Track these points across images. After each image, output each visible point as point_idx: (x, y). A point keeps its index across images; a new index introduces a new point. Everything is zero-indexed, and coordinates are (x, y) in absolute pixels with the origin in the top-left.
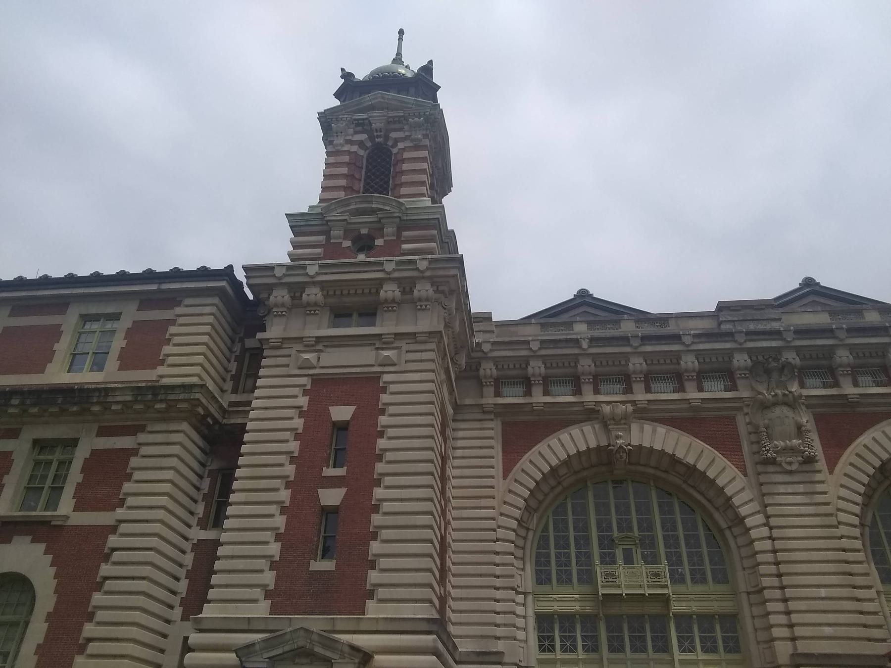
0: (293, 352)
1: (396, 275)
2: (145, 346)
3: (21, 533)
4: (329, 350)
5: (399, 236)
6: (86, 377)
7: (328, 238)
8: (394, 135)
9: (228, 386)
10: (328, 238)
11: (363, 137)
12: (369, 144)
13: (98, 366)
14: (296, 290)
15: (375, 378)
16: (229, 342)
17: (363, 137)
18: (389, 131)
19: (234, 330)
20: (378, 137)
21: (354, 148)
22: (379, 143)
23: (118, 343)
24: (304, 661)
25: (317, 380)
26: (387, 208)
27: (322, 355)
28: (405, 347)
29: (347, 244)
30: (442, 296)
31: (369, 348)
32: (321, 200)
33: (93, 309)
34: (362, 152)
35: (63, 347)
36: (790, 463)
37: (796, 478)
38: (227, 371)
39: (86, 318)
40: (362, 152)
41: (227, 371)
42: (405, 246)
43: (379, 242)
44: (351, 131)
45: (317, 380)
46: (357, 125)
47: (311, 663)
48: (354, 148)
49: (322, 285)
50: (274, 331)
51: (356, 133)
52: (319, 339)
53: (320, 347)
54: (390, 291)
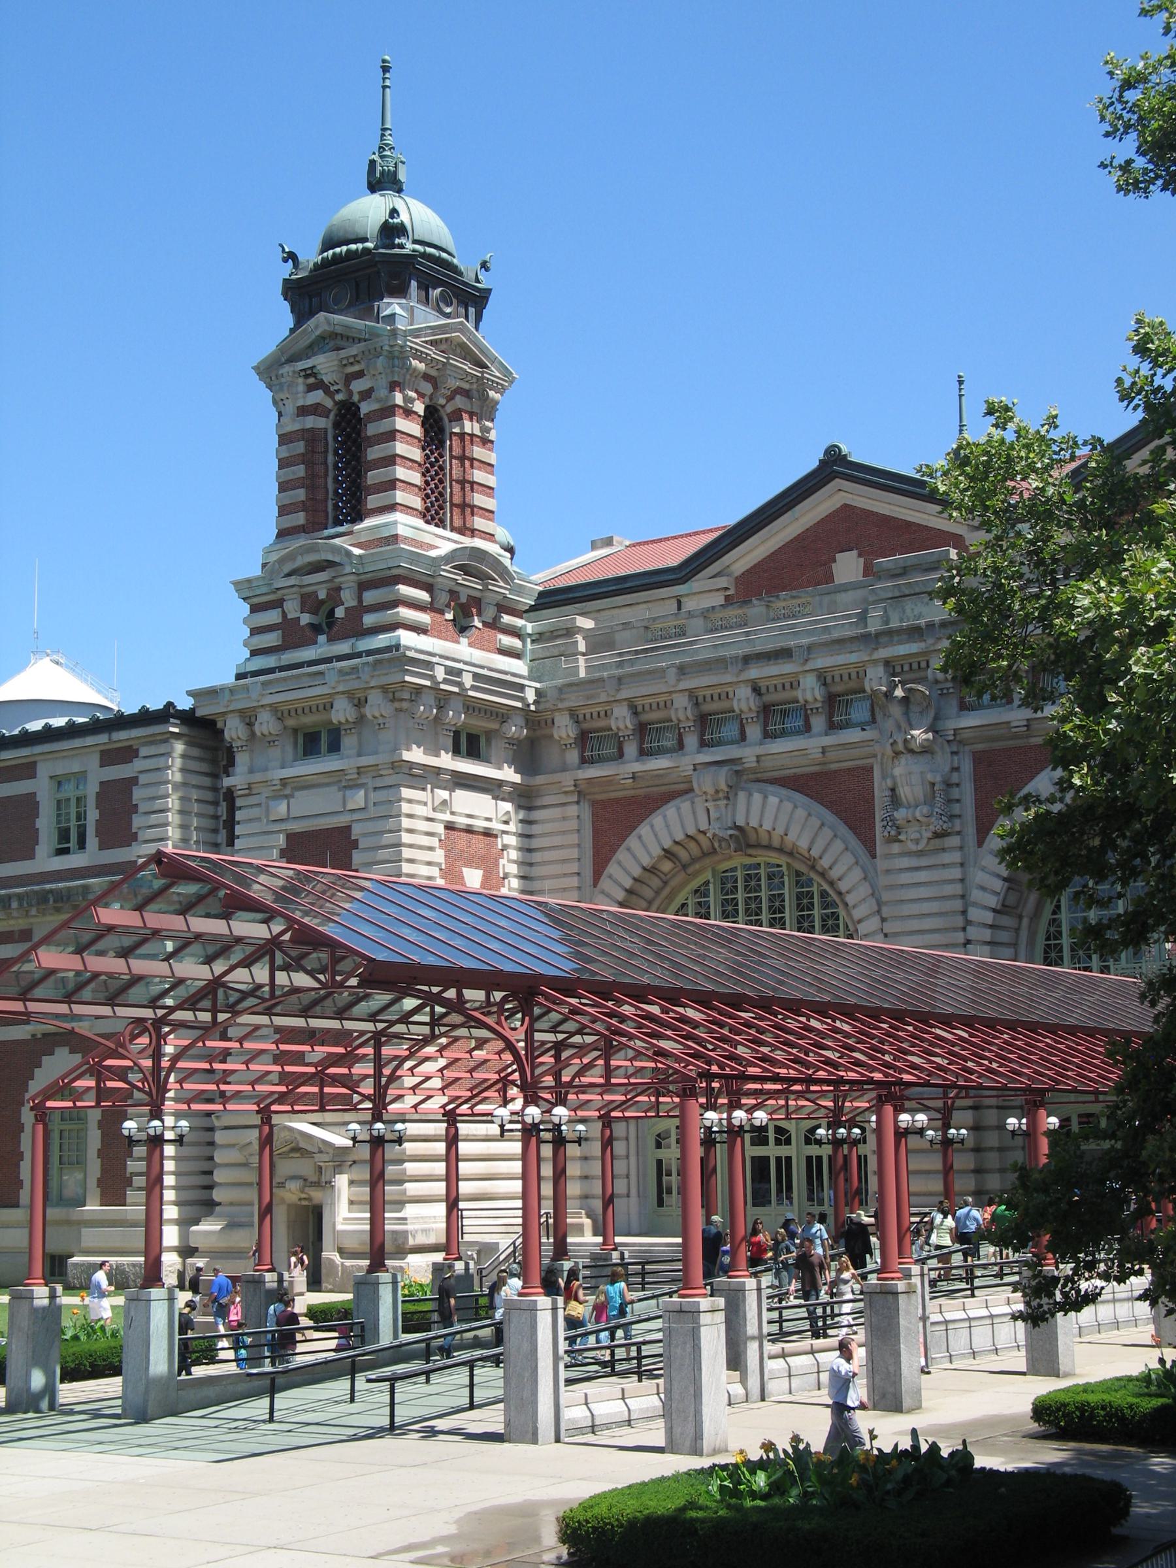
0: (261, 799)
1: (341, 688)
2: (119, 812)
3: (62, 1044)
4: (297, 794)
5: (360, 600)
6: (76, 860)
7: (284, 614)
8: (358, 386)
9: (222, 837)
10: (284, 614)
11: (317, 396)
12: (329, 403)
13: (82, 845)
14: (248, 718)
15: (348, 829)
16: (207, 781)
17: (317, 396)
18: (350, 378)
19: (214, 762)
20: (338, 391)
21: (310, 422)
22: (341, 402)
23: (93, 815)
24: (298, 1155)
25: (291, 837)
26: (337, 559)
27: (292, 800)
28: (371, 783)
29: (305, 619)
30: (405, 705)
31: (336, 788)
32: (282, 534)
33: (61, 768)
34: (321, 423)
35: (46, 824)
36: (917, 841)
37: (924, 862)
38: (216, 817)
39: (59, 781)
40: (321, 423)
41: (216, 817)
42: (369, 620)
43: (340, 613)
44: (301, 388)
45: (291, 837)
46: (307, 376)
47: (302, 1156)
48: (310, 422)
49: (274, 708)
50: (235, 780)
51: (310, 388)
52: (284, 782)
53: (288, 791)
54: (342, 712)
